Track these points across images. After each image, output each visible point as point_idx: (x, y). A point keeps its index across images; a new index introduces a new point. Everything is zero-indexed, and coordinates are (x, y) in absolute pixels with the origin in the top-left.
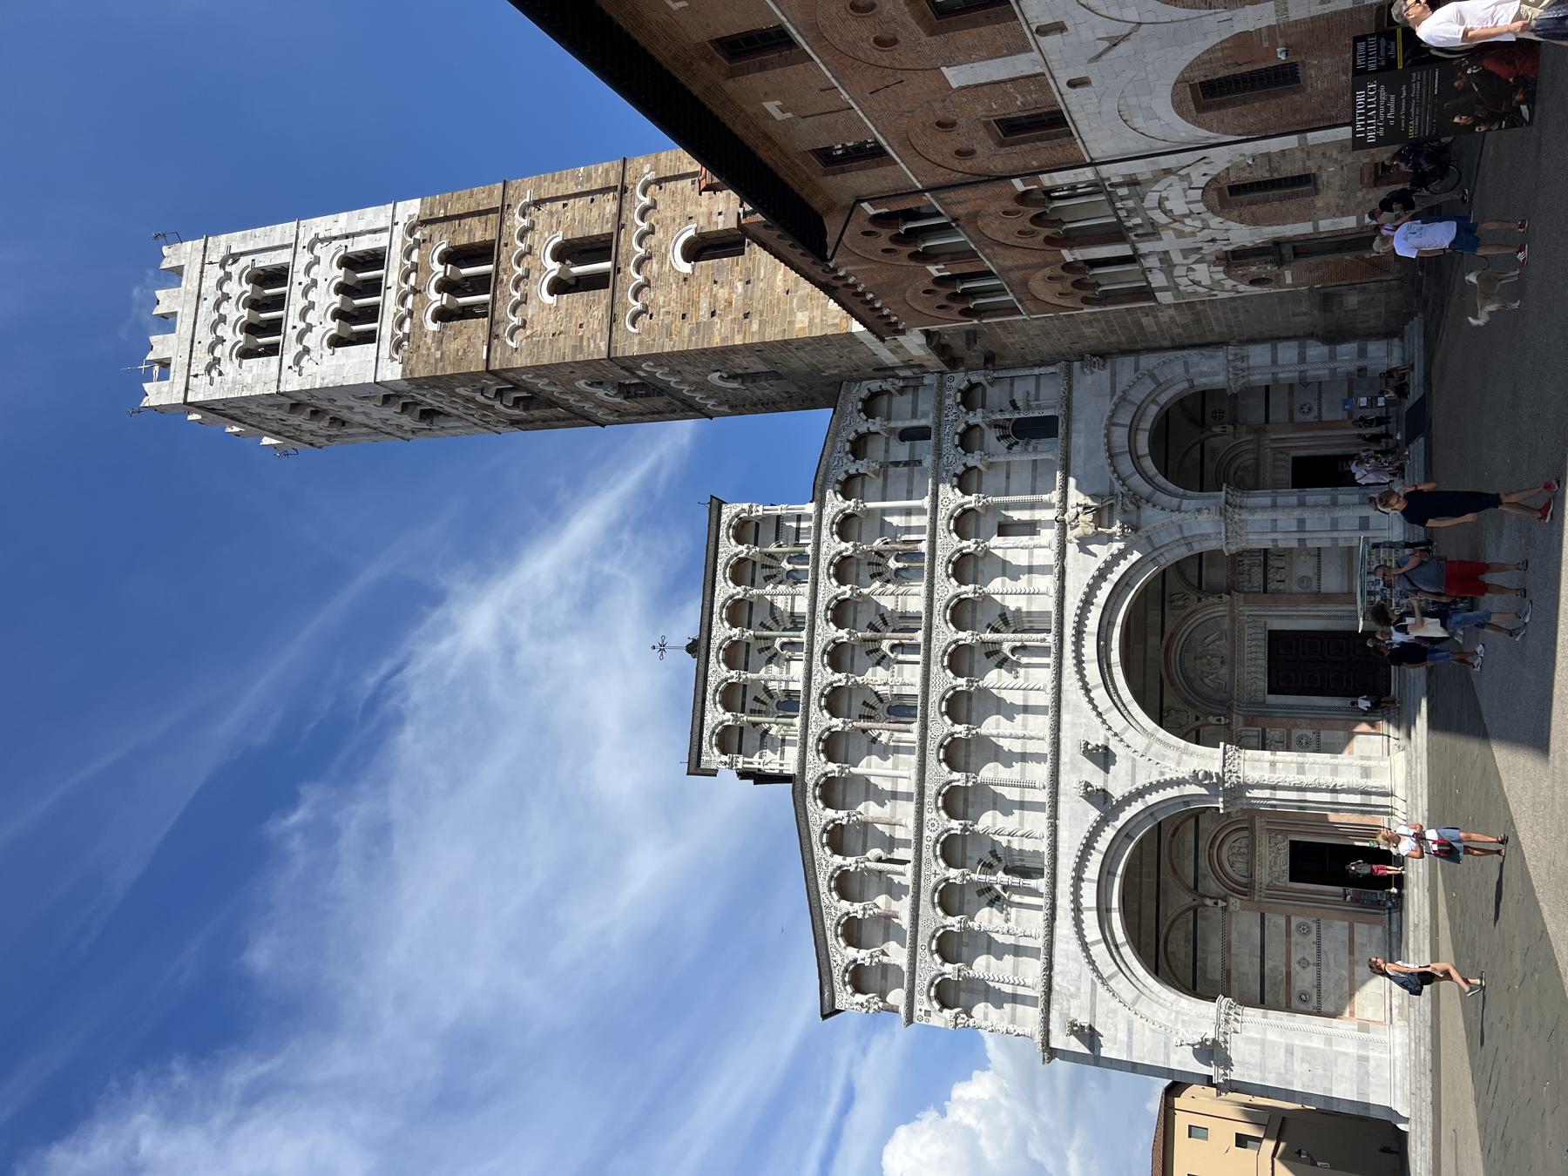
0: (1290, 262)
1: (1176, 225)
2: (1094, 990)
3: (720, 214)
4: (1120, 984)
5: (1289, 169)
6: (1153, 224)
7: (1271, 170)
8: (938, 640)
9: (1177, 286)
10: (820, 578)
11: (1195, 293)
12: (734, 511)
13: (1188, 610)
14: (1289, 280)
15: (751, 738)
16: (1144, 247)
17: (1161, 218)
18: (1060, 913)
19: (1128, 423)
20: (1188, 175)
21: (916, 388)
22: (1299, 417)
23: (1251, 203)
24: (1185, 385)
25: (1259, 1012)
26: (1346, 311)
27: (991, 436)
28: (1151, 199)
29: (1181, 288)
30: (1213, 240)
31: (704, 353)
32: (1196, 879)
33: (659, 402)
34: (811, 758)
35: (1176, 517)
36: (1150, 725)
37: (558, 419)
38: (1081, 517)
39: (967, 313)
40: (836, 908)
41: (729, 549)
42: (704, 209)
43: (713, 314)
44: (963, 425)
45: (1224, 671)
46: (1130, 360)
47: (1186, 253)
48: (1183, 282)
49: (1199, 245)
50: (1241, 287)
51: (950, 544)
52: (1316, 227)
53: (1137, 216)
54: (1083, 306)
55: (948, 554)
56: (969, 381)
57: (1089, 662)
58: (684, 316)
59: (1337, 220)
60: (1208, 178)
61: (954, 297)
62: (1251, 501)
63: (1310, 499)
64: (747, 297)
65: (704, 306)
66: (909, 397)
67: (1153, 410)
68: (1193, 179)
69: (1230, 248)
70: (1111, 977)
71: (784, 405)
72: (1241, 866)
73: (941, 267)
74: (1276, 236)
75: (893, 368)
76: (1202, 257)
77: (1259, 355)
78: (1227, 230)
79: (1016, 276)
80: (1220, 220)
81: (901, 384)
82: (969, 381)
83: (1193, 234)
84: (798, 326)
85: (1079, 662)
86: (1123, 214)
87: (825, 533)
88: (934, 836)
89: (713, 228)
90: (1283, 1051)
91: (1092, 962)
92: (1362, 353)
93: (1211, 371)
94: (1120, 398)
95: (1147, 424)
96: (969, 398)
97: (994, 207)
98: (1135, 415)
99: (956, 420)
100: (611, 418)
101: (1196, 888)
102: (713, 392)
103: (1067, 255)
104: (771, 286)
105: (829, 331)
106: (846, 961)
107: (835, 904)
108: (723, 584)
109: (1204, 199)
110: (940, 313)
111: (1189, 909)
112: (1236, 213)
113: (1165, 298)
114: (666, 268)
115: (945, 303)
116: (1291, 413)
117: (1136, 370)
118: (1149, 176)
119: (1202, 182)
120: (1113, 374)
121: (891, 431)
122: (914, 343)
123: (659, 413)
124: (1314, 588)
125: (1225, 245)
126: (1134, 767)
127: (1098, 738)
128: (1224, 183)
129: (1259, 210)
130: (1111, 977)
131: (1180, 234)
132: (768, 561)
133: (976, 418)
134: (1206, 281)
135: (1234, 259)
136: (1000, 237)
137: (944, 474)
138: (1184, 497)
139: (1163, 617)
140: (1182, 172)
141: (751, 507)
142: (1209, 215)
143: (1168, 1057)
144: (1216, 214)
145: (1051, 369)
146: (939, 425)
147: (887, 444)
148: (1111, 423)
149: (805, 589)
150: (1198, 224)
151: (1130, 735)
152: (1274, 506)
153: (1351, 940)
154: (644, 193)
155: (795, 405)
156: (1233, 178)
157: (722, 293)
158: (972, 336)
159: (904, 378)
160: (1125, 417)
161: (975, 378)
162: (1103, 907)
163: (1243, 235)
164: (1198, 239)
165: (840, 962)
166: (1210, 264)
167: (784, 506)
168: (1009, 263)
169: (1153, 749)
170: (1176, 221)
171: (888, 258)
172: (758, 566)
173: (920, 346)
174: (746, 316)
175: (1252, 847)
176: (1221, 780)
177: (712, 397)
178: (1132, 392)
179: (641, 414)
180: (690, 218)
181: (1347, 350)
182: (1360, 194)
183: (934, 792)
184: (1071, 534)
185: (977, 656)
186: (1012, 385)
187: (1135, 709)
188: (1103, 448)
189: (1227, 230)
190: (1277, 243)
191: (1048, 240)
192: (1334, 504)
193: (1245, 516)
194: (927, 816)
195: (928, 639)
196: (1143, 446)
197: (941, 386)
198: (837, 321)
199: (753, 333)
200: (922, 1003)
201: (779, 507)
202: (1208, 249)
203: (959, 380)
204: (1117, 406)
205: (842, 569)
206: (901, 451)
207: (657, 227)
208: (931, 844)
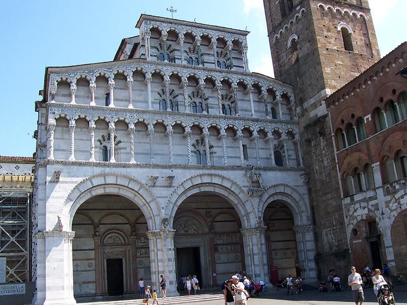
0: (367, 241)
1: (394, 200)
2: (73, 182)
6: (396, 192)
8: (204, 120)
9: (355, 204)
11: (349, 210)
13: (206, 218)
14: (354, 242)
15: (156, 43)
16: (380, 192)
17: (397, 196)
19: (286, 192)
21: (289, 114)
22: (273, 252)
24: (297, 211)
25: (71, 248)
26: (334, 262)
27: (276, 142)
29: (353, 206)
30: (383, 214)
31: (311, 32)
32: (104, 224)
33: (278, 17)
34: (153, 67)
35: (256, 210)
36: (179, 203)
39: (338, 131)
40: (93, 75)
43: (326, 37)
44: (281, 132)
45: (183, 232)
46: (306, 192)
48: (357, 205)
49: (380, 210)
50: (352, 226)
51: (239, 126)
52: (388, 247)
54: (342, 172)
56: (296, 134)
57: (201, 179)
58: (324, 26)
61: (349, 127)
62: (263, 236)
63: (265, 257)
64: (332, 50)
65: (329, 34)
66: (287, 112)
67: (289, 201)
69: (377, 220)
70: (78, 189)
71: (277, 64)
72: (110, 241)
73: (370, 119)
74: (384, 235)
76: (372, 211)
77: (309, 236)
78: (389, 218)
79: (364, 147)
80: (396, 215)
81: (294, 109)
82: (296, 134)
87: (240, 77)
90: (61, 258)
92: (311, 270)
93: (302, 219)
94: (294, 188)
95: (284, 198)
96: (290, 134)
98: (288, 194)
99: (283, 129)
101: (101, 224)
102: (284, 37)
103: (376, 166)
104: (337, 59)
107: (95, 75)
108: (217, 34)
110: (339, 120)
111: (92, 221)
113: (347, 201)
116: (274, 250)
117: (303, 194)
120: (301, 186)
121: (277, 104)
123: (271, 15)
124: (217, 262)
125: (380, 218)
126: (164, 197)
127: (176, 183)
130: (78, 189)
133: (284, 136)
134: (355, 214)
135: (371, 223)
136: (389, 139)
137: (264, 124)
138: (261, 212)
139: (203, 209)
142: (399, 210)
143: (51, 213)
144: (399, 214)
145: (302, 164)
146: (281, 122)
147: (270, 103)
148: (285, 185)
152: (261, 244)
153: (89, 282)
154: (361, 15)
157: (332, 41)
158: (322, 134)
159: (295, 109)
160: (288, 191)
161: (297, 137)
163: (385, 225)
165: (70, 76)
166: (367, 215)
168: (372, 144)
169: (171, 204)
172: (222, 50)
174: (327, 49)
175: (118, 245)
177: (281, 36)
178: (295, 193)
179: (270, 8)
181: (312, 265)
186: (293, 150)
187: (184, 197)
188: (277, 183)
189: (389, 218)
190: (379, 236)
192: (264, 265)
193: (258, 235)
195: (205, 116)
196: (276, 198)
197: (294, 123)
199: (322, 52)
200: (58, 111)
202: (378, 213)
203: (296, 130)
204: (291, 187)
205: (226, 83)
206: (269, 110)
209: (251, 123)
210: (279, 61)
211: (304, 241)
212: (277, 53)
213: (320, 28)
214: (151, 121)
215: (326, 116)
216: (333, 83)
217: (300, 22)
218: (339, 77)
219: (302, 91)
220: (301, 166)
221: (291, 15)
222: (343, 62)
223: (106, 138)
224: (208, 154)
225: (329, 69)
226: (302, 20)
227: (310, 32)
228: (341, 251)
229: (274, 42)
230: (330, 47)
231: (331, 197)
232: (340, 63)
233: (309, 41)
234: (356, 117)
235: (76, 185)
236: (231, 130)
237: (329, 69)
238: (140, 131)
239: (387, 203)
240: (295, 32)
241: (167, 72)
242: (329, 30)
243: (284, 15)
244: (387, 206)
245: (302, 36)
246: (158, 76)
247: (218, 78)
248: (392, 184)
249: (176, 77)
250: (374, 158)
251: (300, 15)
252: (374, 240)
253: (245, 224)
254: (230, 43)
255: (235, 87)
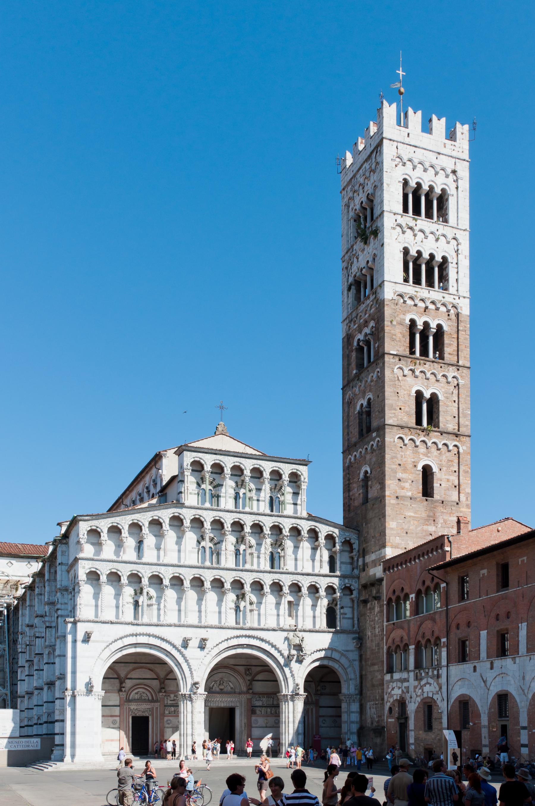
1: (419, 687)
3: (440, 485)
4: (107, 652)
5: (435, 724)
6: (421, 679)
7: (436, 719)
8: (246, 575)
10: (274, 518)
12: (303, 473)
17: (423, 682)
18: (135, 627)
20: (438, 694)
23: (424, 712)
28: (431, 681)
30: (411, 698)
33: (355, 431)
34: (192, 512)
37: (349, 364)
38: (298, 638)
41: (286, 470)
42: (444, 477)
43: (399, 480)
47: (407, 688)
51: (286, 581)
52: (411, 730)
53: (425, 675)
55: (283, 580)
58: (400, 465)
59: (413, 737)
60: (436, 699)
64: (404, 498)
68: (437, 695)
75: (364, 557)
78: (415, 703)
80: (419, 701)
83: (415, 691)
84: (391, 523)
85: (237, 637)
86: (427, 671)
88: (162, 572)
89: (435, 481)
91: (115, 641)
97: (436, 629)
100: (347, 397)
105: (387, 538)
106: (102, 528)
108: (271, 466)
109: (428, 697)
112: (421, 706)
114: (421, 456)
115: (396, 594)
118: (440, 681)
119: (435, 697)
122: (378, 571)
123: (348, 426)
128: (433, 704)
129: (421, 715)
131: (415, 687)
132: (278, 488)
140: (439, 692)
141: (306, 482)
142: (422, 697)
144: (422, 700)
149: (268, 511)
150: (419, 694)
151: (209, 658)
155: (347, 500)
156: (434, 707)
157: (407, 485)
162: (137, 645)
163: (412, 708)
164: (413, 693)
167: (305, 500)
170: (421, 687)
171: (420, 582)
172: (276, 482)
173: (375, 574)
174: (397, 497)
176: (195, 693)
180: (440, 470)
182: (422, 744)
183: (181, 572)
184: (291, 634)
185: (237, 591)
189: (415, 703)
190: (407, 719)
191: (419, 642)
194: (170, 568)
198: (391, 541)
199: (390, 501)
201: (305, 497)
202: (408, 696)
207: (439, 452)
208: (158, 571)
209: (299, 578)
210: (349, 491)
211: (349, 712)
212: (349, 480)
213: (392, 470)
214: (187, 575)
215: (381, 580)
216: (398, 540)
217: (374, 454)
218: (407, 533)
219: (366, 541)
220: (355, 629)
221: (367, 440)
222: (415, 513)
223: (139, 591)
224: (248, 611)
225: (395, 523)
226: (377, 452)
227: (381, 472)
228: (379, 728)
229: (347, 465)
230: (401, 493)
231: (377, 669)
232: (412, 514)
233: (379, 483)
234: (405, 592)
235: (108, 644)
236: (277, 587)
237: (395, 523)
238: (175, 585)
239: (415, 687)
240: (369, 463)
241: (208, 517)
242: (405, 470)
243: (361, 434)
244: (415, 691)
245: (373, 472)
246: (198, 522)
247: (268, 523)
248: (420, 671)
249: (218, 524)
250: (411, 641)
251: (375, 445)
252: (402, 721)
253: (284, 692)
254: (286, 478)
255: (286, 534)
